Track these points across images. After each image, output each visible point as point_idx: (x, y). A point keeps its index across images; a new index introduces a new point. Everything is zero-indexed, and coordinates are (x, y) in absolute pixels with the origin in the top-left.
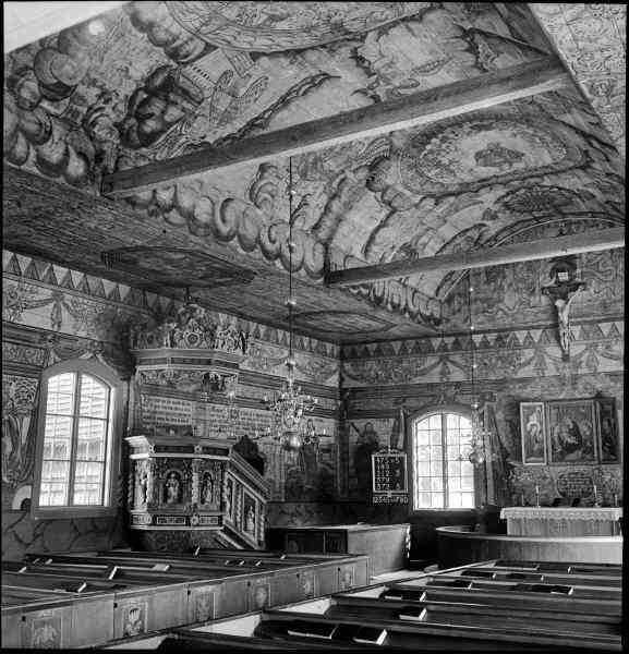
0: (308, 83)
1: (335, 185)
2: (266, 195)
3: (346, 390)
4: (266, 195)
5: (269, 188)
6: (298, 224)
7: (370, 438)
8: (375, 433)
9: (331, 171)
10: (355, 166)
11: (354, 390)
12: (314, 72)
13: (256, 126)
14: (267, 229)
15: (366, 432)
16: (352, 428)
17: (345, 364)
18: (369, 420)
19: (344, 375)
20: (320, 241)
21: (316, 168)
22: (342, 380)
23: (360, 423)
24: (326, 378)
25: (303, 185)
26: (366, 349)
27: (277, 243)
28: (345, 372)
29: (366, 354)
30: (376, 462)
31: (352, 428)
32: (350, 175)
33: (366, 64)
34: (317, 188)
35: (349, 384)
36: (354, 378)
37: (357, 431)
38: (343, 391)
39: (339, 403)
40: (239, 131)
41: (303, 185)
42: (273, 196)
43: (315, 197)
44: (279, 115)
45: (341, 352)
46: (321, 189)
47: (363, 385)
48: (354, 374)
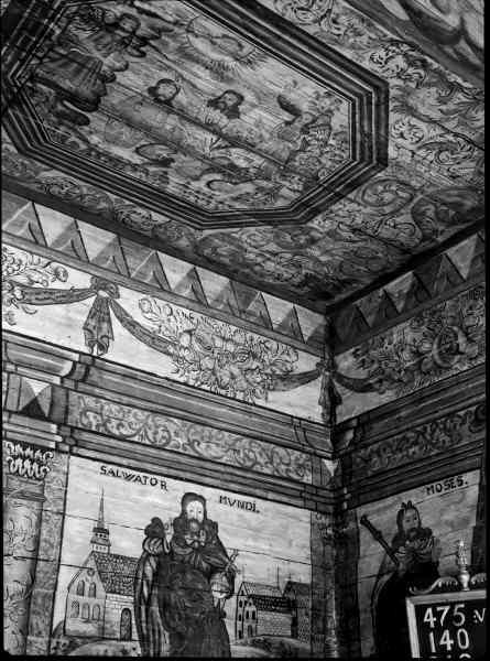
3: (345, 426)
7: (414, 553)
8: (427, 533)
11: (365, 421)
15: (400, 538)
16: (365, 535)
17: (338, 359)
18: (406, 497)
19: (339, 388)
22: (332, 401)
23: (383, 513)
24: (267, 388)
26: (385, 291)
28: (341, 378)
29: (389, 314)
30: (423, 628)
31: (365, 535)
35: (354, 405)
36: (363, 387)
37: (378, 536)
38: (337, 431)
39: (330, 466)
45: (331, 329)
47: (388, 396)
48: (362, 374)
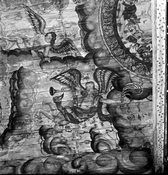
0: (14, 83)
1: (104, 112)
2: (59, 145)
4: (59, 145)
5: (58, 140)
6: (103, 148)
9: (91, 108)
10: (105, 96)
12: (10, 76)
13: (15, 117)
14: (70, 163)
20: (137, 149)
21: (80, 113)
25: (81, 126)
27: (83, 167)
32: (110, 102)
33: (18, 51)
34: (94, 122)
40: (8, 125)
41: (81, 126)
42: (64, 143)
43: (99, 126)
44: (21, 105)
46: (98, 120)
